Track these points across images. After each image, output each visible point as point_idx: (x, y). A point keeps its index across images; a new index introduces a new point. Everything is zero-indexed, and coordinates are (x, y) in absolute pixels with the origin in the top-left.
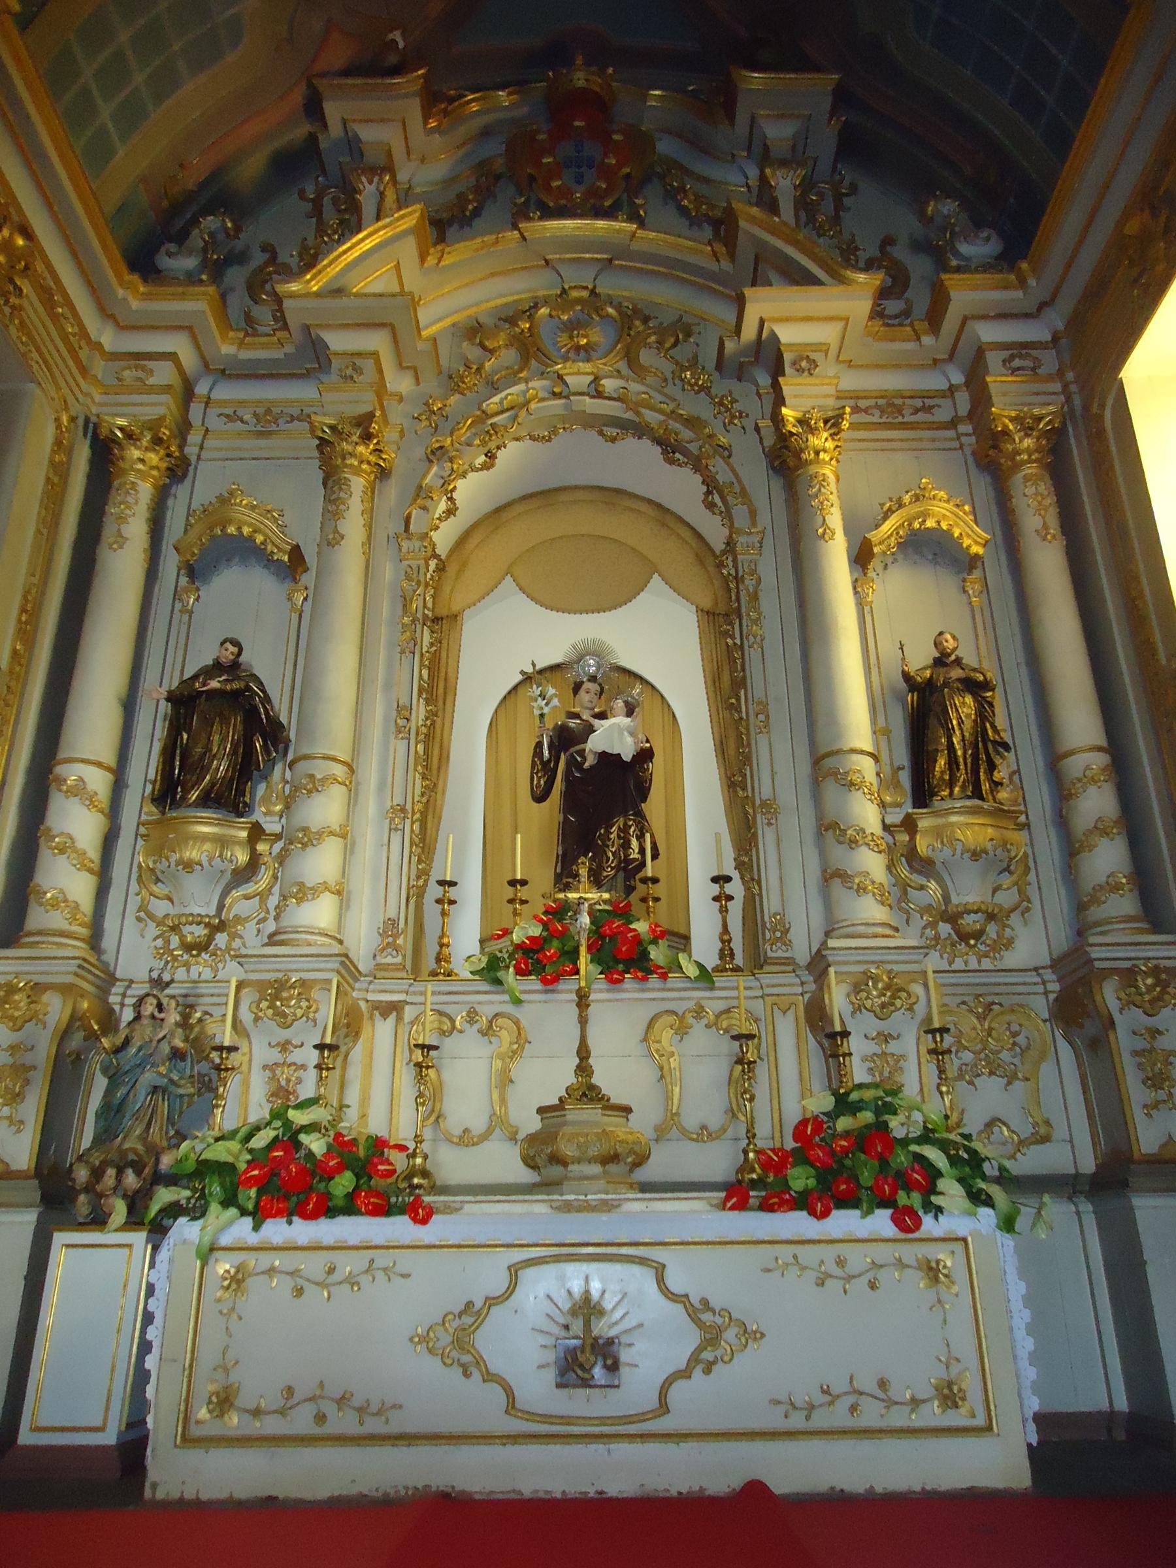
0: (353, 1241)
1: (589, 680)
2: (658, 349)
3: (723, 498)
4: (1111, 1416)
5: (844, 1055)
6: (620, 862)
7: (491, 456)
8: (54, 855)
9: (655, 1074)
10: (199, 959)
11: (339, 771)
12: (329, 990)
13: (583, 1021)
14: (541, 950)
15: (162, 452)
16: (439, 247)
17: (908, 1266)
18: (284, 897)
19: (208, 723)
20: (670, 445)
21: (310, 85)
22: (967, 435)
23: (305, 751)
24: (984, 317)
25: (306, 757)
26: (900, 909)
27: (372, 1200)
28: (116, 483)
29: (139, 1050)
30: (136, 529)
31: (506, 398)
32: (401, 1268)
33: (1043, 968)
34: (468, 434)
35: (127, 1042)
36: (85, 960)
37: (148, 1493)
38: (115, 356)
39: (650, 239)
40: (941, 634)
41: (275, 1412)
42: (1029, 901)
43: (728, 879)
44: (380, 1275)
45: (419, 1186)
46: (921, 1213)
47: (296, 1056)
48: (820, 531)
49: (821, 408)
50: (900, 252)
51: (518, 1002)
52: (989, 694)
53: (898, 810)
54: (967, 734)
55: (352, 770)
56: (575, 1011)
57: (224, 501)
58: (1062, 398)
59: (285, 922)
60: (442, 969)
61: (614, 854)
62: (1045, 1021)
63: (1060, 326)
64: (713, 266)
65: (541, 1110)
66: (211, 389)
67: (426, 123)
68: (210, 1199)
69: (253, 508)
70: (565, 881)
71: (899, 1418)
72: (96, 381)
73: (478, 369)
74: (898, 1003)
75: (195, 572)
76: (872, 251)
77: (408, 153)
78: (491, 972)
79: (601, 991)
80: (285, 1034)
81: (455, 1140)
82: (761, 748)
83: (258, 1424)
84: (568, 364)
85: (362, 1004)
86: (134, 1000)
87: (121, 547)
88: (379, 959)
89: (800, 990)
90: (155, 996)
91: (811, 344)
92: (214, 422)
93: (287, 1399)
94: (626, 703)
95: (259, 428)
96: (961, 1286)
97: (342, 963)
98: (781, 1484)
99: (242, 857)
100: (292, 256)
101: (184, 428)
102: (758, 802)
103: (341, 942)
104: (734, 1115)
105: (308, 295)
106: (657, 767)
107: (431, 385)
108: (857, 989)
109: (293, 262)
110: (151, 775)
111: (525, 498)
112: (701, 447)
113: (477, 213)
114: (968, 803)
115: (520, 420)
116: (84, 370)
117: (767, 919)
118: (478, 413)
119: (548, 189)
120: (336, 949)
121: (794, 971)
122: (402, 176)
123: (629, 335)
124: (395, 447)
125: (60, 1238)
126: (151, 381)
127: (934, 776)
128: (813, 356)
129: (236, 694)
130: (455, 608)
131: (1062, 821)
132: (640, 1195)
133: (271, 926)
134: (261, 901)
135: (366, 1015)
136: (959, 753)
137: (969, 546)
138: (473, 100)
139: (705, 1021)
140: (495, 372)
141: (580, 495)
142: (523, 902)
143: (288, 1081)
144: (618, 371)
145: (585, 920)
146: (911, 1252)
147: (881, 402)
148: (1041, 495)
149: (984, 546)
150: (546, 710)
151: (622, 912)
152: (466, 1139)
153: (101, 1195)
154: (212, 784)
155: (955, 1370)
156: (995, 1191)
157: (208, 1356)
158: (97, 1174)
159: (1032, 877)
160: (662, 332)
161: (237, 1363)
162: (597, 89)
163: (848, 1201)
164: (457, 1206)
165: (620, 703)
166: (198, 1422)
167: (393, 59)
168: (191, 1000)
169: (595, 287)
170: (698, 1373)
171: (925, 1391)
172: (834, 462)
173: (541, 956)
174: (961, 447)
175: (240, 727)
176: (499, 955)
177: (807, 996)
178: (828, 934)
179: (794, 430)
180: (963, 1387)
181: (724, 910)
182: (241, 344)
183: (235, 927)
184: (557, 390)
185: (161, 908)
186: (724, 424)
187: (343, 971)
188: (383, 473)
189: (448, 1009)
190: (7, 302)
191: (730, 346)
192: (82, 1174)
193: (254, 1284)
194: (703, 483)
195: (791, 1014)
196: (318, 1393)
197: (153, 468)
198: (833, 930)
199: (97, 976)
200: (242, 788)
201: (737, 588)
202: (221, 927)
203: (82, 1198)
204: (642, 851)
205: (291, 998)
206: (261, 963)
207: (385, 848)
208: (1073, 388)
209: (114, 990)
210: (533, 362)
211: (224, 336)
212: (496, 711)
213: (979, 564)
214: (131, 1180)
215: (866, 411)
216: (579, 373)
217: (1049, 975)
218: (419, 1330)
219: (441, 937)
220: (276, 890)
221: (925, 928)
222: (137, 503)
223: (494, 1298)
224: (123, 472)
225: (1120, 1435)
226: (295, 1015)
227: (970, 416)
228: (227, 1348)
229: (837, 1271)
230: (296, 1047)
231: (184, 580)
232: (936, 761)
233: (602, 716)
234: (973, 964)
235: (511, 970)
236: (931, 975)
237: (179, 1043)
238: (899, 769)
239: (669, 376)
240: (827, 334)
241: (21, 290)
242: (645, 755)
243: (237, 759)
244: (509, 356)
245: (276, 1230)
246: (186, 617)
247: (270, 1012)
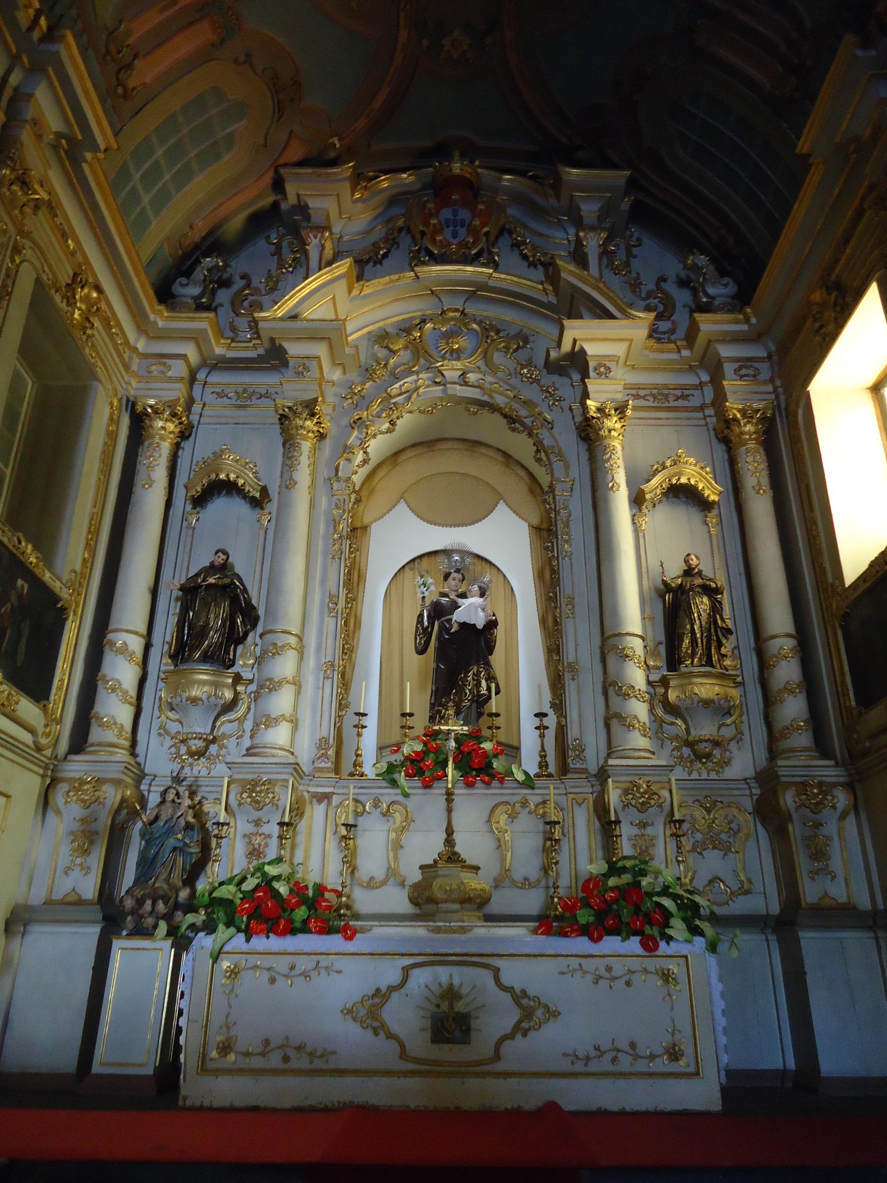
0: (307, 949)
1: (455, 572)
2: (505, 352)
3: (548, 459)
4: (784, 1073)
5: (617, 836)
6: (474, 697)
7: (392, 423)
8: (109, 693)
10: (199, 762)
11: (293, 641)
12: (287, 787)
13: (449, 811)
14: (422, 760)
15: (177, 422)
16: (361, 283)
17: (651, 973)
18: (256, 725)
19: (206, 606)
20: (512, 418)
21: (276, 171)
22: (710, 416)
23: (270, 627)
25: (271, 632)
26: (658, 738)
27: (319, 924)
28: (146, 443)
29: (166, 823)
30: (160, 475)
31: (403, 385)
32: (336, 967)
33: (750, 779)
34: (378, 409)
35: (157, 818)
36: (129, 764)
37: (181, 1103)
38: (145, 356)
39: (501, 279)
40: (689, 555)
41: (258, 1054)
42: (742, 734)
43: (545, 715)
44: (323, 972)
45: (344, 915)
46: (658, 939)
47: (265, 829)
48: (610, 485)
49: (613, 401)
50: (670, 287)
51: (406, 795)
52: (719, 596)
53: (657, 671)
54: (703, 623)
55: (300, 638)
56: (444, 804)
57: (218, 455)
58: (773, 396)
59: (257, 741)
60: (356, 773)
61: (470, 690)
62: (750, 814)
63: (773, 348)
64: (544, 299)
65: (422, 867)
66: (206, 377)
68: (218, 922)
69: (237, 461)
70: (436, 708)
71: (642, 1066)
72: (135, 375)
73: (385, 364)
74: (652, 802)
75: (199, 501)
76: (652, 286)
77: (340, 213)
78: (389, 775)
79: (461, 788)
80: (257, 814)
81: (365, 884)
82: (569, 627)
83: (248, 1061)
84: (446, 362)
85: (306, 795)
86: (162, 789)
87: (150, 486)
88: (317, 765)
89: (590, 790)
90: (175, 788)
91: (609, 356)
92: (209, 398)
93: (265, 1047)
94: (480, 587)
95: (238, 402)
96: (683, 985)
97: (295, 769)
98: (569, 1104)
99: (228, 695)
100: (261, 282)
101: (190, 403)
102: (566, 664)
103: (293, 754)
105: (274, 319)
106: (500, 633)
107: (353, 375)
108: (626, 792)
109: (262, 287)
110: (168, 638)
111: (414, 446)
112: (533, 422)
113: (385, 256)
114: (703, 669)
115: (412, 400)
116: (127, 367)
117: (570, 742)
118: (385, 395)
119: (434, 241)
120: (292, 760)
121: (587, 778)
122: (336, 229)
123: (486, 342)
124: (329, 418)
125: (119, 946)
126: (170, 373)
127: (682, 651)
128: (608, 364)
129: (225, 587)
130: (366, 521)
131: (764, 683)
132: (484, 924)
133: (247, 742)
134: (239, 722)
135: (307, 801)
136: (698, 635)
137: (709, 496)
138: (384, 180)
140: (396, 367)
141: (450, 445)
142: (410, 728)
143: (260, 845)
144: (479, 368)
145: (453, 744)
146: (652, 964)
147: (655, 392)
148: (757, 462)
149: (719, 495)
150: (426, 594)
151: (476, 736)
152: (371, 884)
153: (142, 917)
154: (209, 646)
155: (677, 1037)
156: (705, 926)
157: (217, 1020)
158: (140, 902)
159: (745, 718)
160: (509, 338)
161: (235, 1023)
162: (468, 176)
163: (614, 931)
165: (475, 588)
166: (211, 1060)
167: (332, 155)
168: (194, 788)
169: (464, 309)
170: (519, 1036)
171: (658, 1050)
172: (620, 437)
173: (422, 764)
174: (707, 424)
175: (227, 609)
176: (395, 763)
177: (595, 795)
178: (609, 756)
179: (595, 415)
180: (682, 1048)
181: (542, 736)
182: (229, 347)
183: (223, 740)
184: (437, 380)
185: (174, 727)
186: (549, 407)
187: (295, 774)
188: (321, 437)
189: (361, 798)
190: (84, 333)
191: (553, 354)
192: (129, 903)
193: (246, 975)
194: (534, 444)
195: (584, 806)
196: (285, 1042)
197: (170, 433)
198: (611, 753)
199: (135, 774)
200: (228, 649)
201: (556, 517)
202: (214, 741)
203: (129, 918)
204: (489, 689)
205: (261, 792)
206: (242, 768)
207: (321, 690)
208: (780, 390)
209: (144, 781)
210: (422, 361)
211: (218, 342)
213: (716, 506)
214: (161, 907)
215: (644, 397)
216: (453, 369)
217: (753, 784)
218: (347, 1006)
219: (357, 750)
220: (251, 716)
221: (673, 750)
222: (160, 456)
223: (393, 987)
224: (152, 436)
225: (789, 1085)
227: (713, 404)
228: (229, 1014)
229: (608, 976)
230: (265, 823)
231: (189, 507)
232: (683, 641)
233: (463, 596)
234: (704, 776)
235: (403, 773)
236: (673, 782)
237: (191, 819)
238: (660, 643)
239: (512, 370)
240: (619, 350)
241: (93, 325)
242: (492, 624)
243: (225, 629)
244: (405, 356)
245: (259, 943)
246: (190, 531)
247: (249, 800)
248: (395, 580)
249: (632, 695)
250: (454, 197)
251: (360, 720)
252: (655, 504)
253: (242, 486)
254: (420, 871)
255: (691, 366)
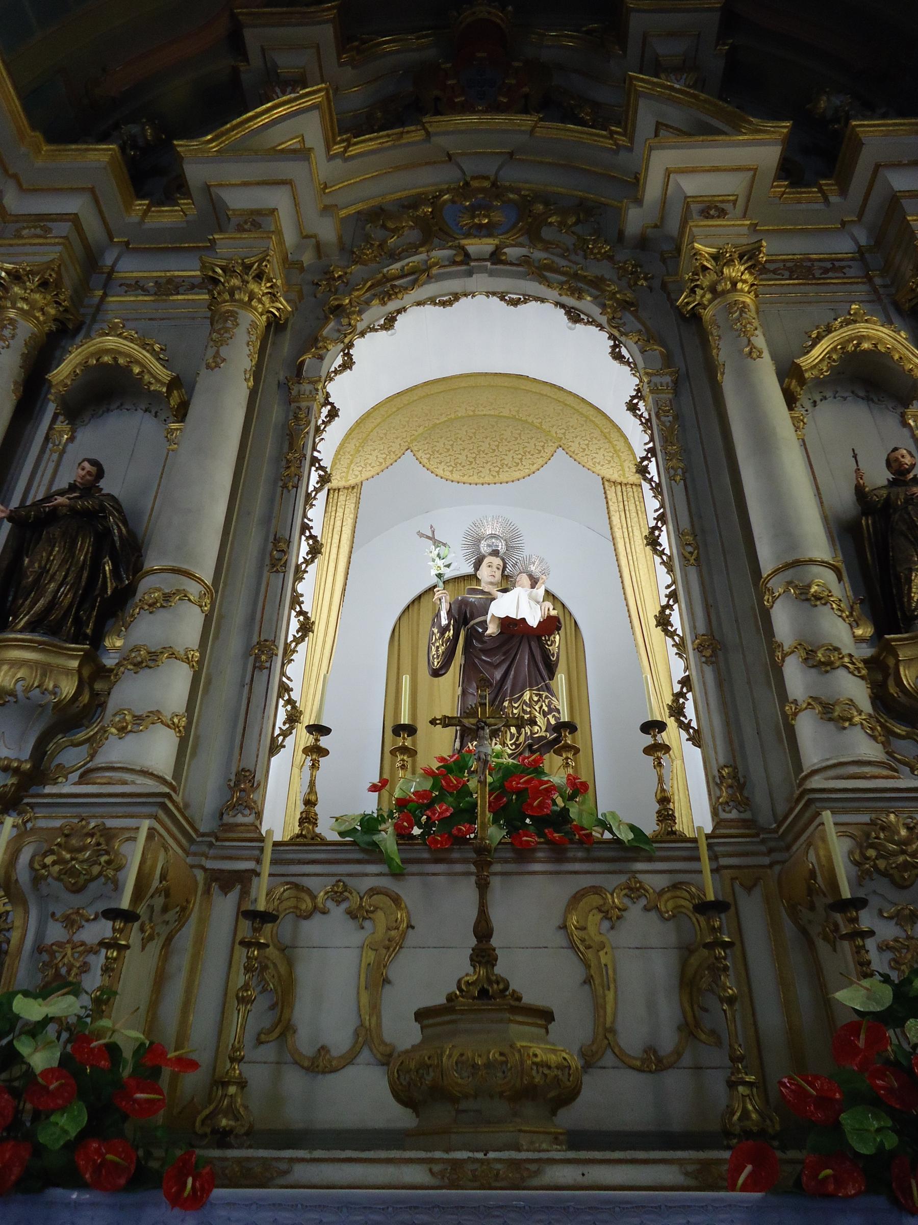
9: (579, 973)
24: (897, 165)
31: (408, 264)
40: (895, 449)
43: (661, 726)
65: (421, 1015)
67: (339, 57)
73: (380, 245)
79: (506, 861)
104: (691, 1033)
132: (571, 1155)
139: (643, 902)
164: (283, 1166)
194: (609, 338)
195: (757, 892)
207: (247, 688)
212: (400, 618)
226: (88, 872)
230: (88, 920)
239: (571, 247)
244: (412, 235)
248: (406, 613)
249: (838, 664)
250: (479, 55)
251: (317, 740)
252: (815, 402)
253: (138, 374)
254: (417, 1026)
255: (843, 224)
